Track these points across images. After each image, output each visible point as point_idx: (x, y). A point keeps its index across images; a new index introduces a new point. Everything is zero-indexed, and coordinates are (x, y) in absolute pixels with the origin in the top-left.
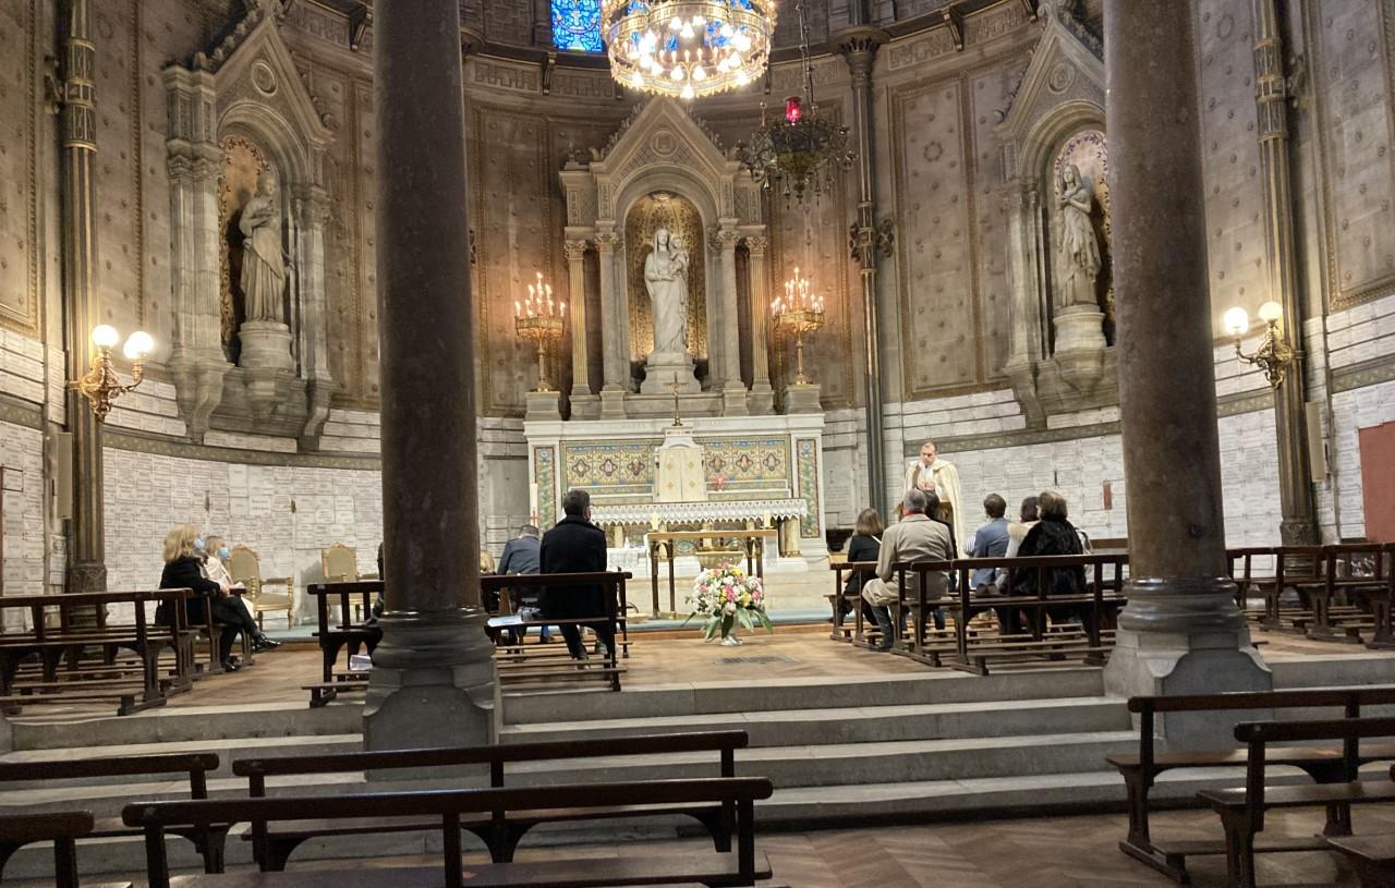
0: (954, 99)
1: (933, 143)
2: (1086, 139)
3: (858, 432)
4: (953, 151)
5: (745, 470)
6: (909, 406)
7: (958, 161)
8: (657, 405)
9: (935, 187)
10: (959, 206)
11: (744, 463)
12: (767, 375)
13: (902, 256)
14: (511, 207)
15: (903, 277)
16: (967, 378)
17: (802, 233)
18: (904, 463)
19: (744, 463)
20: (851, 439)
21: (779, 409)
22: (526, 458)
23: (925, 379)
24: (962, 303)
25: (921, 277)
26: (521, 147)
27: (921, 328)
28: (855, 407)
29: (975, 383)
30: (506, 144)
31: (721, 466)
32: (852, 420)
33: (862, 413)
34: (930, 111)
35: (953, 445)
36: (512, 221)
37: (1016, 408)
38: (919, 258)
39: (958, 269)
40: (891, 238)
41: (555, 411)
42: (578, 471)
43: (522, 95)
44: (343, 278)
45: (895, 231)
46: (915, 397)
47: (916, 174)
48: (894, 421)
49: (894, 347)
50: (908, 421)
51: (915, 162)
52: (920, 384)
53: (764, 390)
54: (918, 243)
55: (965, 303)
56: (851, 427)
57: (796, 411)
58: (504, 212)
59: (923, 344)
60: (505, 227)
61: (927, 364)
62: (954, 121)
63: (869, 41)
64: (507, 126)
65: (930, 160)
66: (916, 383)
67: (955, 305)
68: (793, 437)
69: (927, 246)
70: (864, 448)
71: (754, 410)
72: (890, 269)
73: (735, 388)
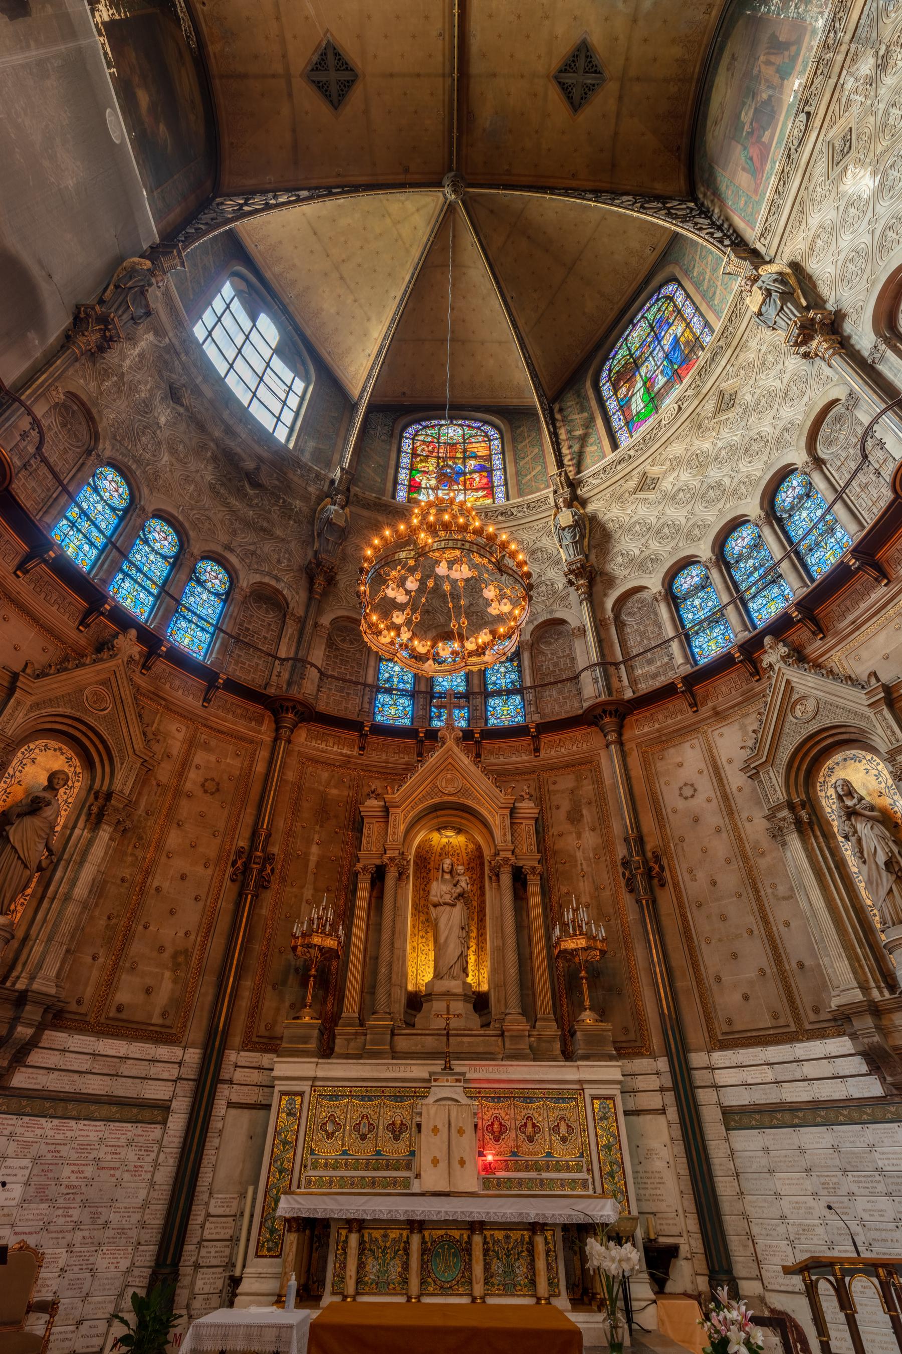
0: (698, 748)
1: (686, 784)
2: (845, 760)
3: (662, 1090)
4: (706, 787)
5: (531, 1140)
6: (720, 1058)
7: (713, 796)
8: (430, 1043)
9: (696, 820)
10: (724, 835)
11: (529, 1130)
12: (551, 1010)
13: (676, 885)
14: (316, 837)
15: (681, 906)
16: (782, 1022)
17: (576, 866)
18: (727, 1140)
19: (529, 1130)
20: (655, 1101)
21: (568, 1055)
22: (268, 1107)
23: (730, 1022)
24: (752, 932)
25: (700, 906)
26: (334, 792)
27: (712, 959)
28: (655, 1058)
29: (793, 1028)
30: (321, 788)
31: (501, 1133)
32: (651, 1072)
33: (662, 1064)
34: (679, 760)
35: (787, 1117)
36: (314, 849)
37: (858, 1065)
38: (694, 886)
39: (740, 896)
40: (662, 868)
41: (312, 1046)
42: (326, 1131)
43: (342, 755)
44: (126, 885)
45: (665, 862)
46: (724, 1045)
47: (675, 811)
48: (700, 1077)
49: (684, 983)
50: (723, 1077)
51: (671, 799)
52: (725, 1028)
53: (551, 1029)
54: (691, 871)
55: (756, 932)
56: (654, 1083)
57: (586, 1057)
58: (309, 842)
59: (718, 979)
60: (307, 854)
61: (728, 1000)
62: (703, 766)
63: (616, 711)
64: (325, 775)
65: (686, 798)
66: (721, 1027)
67: (745, 935)
68: (588, 1093)
69: (701, 875)
70: (672, 1113)
71: (537, 1055)
72: (666, 900)
73: (516, 1023)
